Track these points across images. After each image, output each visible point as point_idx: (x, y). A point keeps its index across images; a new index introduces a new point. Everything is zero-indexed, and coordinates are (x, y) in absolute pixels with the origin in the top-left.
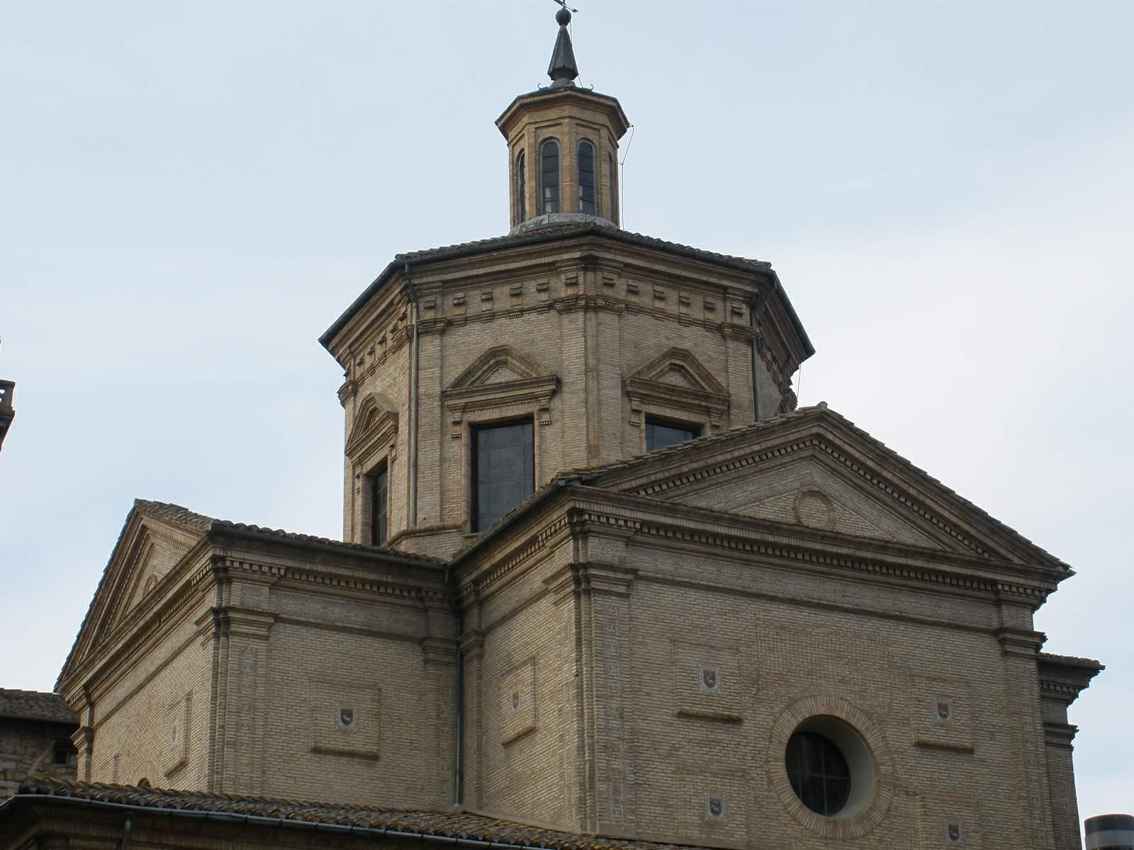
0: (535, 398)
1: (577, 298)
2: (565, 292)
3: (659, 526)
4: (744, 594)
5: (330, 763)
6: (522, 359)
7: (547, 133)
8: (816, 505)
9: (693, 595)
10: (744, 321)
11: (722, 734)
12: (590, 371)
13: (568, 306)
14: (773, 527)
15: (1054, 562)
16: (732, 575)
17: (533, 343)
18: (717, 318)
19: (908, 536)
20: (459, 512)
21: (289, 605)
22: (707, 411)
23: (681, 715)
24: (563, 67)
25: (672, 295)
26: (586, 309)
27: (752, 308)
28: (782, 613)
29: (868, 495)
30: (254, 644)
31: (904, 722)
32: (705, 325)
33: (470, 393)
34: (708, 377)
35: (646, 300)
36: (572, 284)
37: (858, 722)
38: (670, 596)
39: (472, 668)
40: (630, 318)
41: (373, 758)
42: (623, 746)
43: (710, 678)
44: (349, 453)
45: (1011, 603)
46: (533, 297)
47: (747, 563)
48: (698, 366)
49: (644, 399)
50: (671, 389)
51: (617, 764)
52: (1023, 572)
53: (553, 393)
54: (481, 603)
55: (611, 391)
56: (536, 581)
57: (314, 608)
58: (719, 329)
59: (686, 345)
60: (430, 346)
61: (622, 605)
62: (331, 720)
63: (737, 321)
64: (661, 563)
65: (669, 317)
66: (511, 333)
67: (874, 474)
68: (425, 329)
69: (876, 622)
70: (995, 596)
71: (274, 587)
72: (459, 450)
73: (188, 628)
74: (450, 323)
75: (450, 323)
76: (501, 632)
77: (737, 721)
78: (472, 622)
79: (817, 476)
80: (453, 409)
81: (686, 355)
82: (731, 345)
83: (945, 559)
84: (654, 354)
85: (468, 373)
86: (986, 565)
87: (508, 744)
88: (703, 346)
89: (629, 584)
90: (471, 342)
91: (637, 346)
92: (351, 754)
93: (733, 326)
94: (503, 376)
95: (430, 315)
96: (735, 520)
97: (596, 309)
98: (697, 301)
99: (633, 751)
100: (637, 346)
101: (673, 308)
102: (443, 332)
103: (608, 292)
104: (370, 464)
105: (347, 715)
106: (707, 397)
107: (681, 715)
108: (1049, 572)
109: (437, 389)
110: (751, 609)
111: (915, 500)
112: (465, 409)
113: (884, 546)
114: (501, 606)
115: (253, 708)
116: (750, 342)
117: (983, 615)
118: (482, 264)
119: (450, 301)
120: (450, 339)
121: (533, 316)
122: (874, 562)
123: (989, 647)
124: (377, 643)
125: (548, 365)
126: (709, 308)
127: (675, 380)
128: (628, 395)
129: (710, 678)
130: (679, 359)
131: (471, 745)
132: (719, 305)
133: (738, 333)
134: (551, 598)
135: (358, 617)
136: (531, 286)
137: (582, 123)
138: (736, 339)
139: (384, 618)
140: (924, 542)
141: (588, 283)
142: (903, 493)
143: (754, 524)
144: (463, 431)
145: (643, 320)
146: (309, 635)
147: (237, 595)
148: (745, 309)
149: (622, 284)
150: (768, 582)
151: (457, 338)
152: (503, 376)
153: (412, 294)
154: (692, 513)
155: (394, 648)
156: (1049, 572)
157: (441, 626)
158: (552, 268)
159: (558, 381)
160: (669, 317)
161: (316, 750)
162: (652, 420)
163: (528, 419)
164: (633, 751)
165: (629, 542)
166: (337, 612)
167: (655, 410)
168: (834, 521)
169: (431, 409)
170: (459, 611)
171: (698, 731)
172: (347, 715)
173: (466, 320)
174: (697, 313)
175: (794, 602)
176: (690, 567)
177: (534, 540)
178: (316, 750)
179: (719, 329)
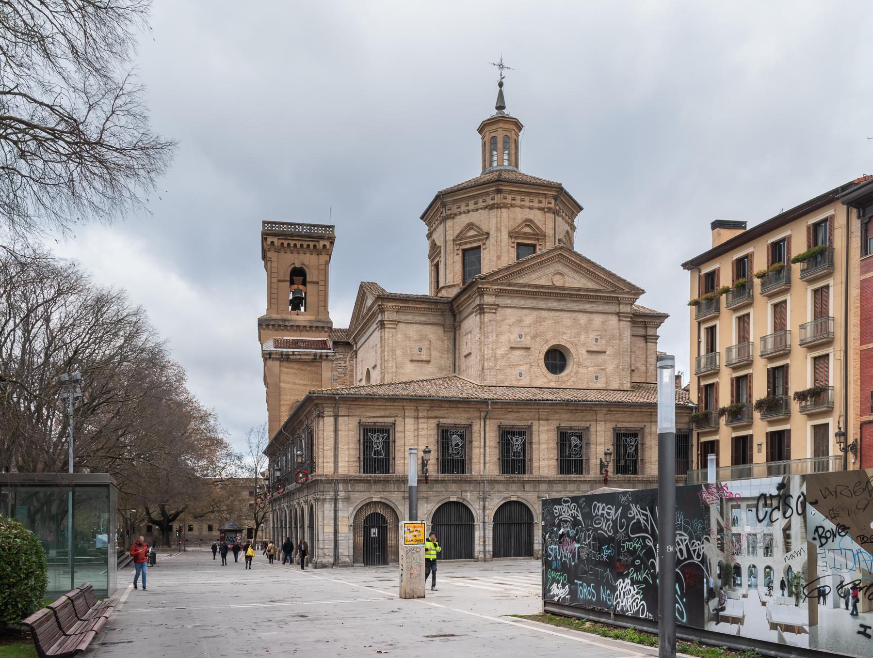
0: (481, 240)
1: (494, 204)
2: (491, 202)
3: (506, 290)
4: (533, 309)
5: (415, 364)
6: (477, 227)
7: (493, 135)
8: (559, 277)
9: (516, 310)
10: (552, 206)
11: (524, 353)
12: (498, 230)
13: (491, 207)
14: (542, 287)
15: (639, 289)
16: (530, 303)
17: (481, 221)
18: (542, 205)
19: (591, 285)
20: (459, 280)
21: (402, 317)
22: (538, 239)
23: (511, 348)
24: (500, 107)
25: (527, 199)
26: (497, 208)
27: (556, 200)
28: (545, 313)
29: (577, 272)
30: (392, 330)
31: (584, 345)
32: (539, 209)
33: (461, 239)
34: (538, 228)
35: (518, 202)
36: (493, 199)
37: (568, 346)
38: (509, 311)
39: (457, 332)
40: (512, 209)
41: (428, 362)
42: (492, 359)
43: (521, 336)
44: (429, 258)
45: (623, 303)
46: (481, 204)
47: (535, 299)
48: (535, 224)
49: (516, 238)
50: (525, 233)
51: (491, 364)
52: (627, 293)
53: (487, 238)
54: (460, 312)
55: (505, 236)
56: (470, 310)
57: (410, 318)
58: (543, 209)
59: (531, 217)
60: (449, 223)
61: (493, 316)
62: (416, 351)
63: (549, 205)
64: (507, 301)
65: (526, 207)
66: (475, 218)
67: (579, 265)
68: (449, 217)
69: (577, 314)
70: (618, 302)
71: (397, 312)
72: (459, 259)
73: (374, 326)
74: (456, 215)
75: (456, 215)
76: (464, 322)
77: (529, 348)
78: (458, 318)
79: (559, 267)
80: (457, 245)
81: (531, 221)
82: (547, 215)
83: (600, 291)
84: (520, 221)
85: (461, 232)
86: (614, 292)
87: (466, 357)
88: (536, 216)
89: (496, 309)
90: (462, 221)
91: (514, 219)
92: (422, 361)
93: (548, 208)
94: (472, 233)
95: (449, 212)
96: (530, 286)
97: (501, 208)
98: (536, 200)
99: (496, 360)
100: (514, 219)
101: (527, 203)
102: (453, 218)
103: (504, 201)
104: (435, 262)
105: (420, 350)
106: (537, 235)
107: (511, 348)
108: (638, 292)
109: (452, 238)
110: (535, 313)
111: (592, 272)
112: (460, 245)
113: (580, 289)
114: (465, 314)
115: (392, 350)
116: (554, 213)
117: (613, 308)
118: (465, 193)
119: (455, 207)
120: (455, 220)
121: (481, 211)
122: (577, 295)
123: (615, 318)
124: (429, 327)
125: (485, 229)
126: (540, 202)
127: (527, 230)
128: (511, 237)
129: (521, 336)
130: (528, 222)
131: (457, 356)
132: (544, 200)
133: (549, 210)
134: (474, 315)
135: (423, 319)
136: (480, 200)
137: (505, 130)
138: (549, 212)
139: (431, 319)
140: (596, 287)
141: (498, 199)
142: (588, 270)
143: (536, 286)
144: (460, 253)
145: (517, 209)
146: (409, 326)
147: (387, 316)
148: (553, 201)
149: (509, 197)
150: (542, 304)
151: (458, 218)
152: (472, 233)
153: (444, 205)
154: (516, 285)
155: (434, 328)
156: (638, 292)
157: (449, 320)
158: (487, 194)
159: (488, 234)
160: (526, 207)
161: (412, 361)
162: (519, 244)
163: (479, 247)
164: (496, 360)
165: (496, 296)
166: (417, 318)
167: (520, 241)
168: (564, 282)
169: (450, 244)
170: (454, 316)
171: (516, 352)
172: (420, 350)
173: (461, 213)
174: (536, 204)
175: (549, 310)
176: (516, 302)
177: (470, 296)
178: (412, 361)
179: (543, 209)
